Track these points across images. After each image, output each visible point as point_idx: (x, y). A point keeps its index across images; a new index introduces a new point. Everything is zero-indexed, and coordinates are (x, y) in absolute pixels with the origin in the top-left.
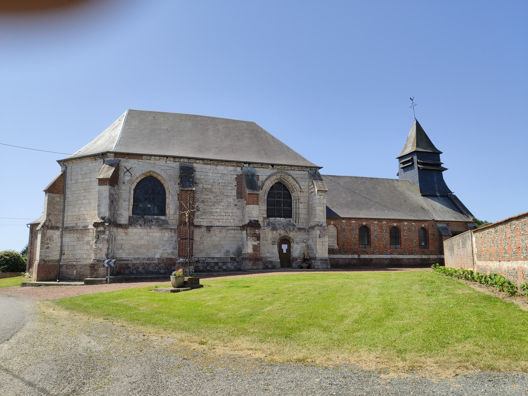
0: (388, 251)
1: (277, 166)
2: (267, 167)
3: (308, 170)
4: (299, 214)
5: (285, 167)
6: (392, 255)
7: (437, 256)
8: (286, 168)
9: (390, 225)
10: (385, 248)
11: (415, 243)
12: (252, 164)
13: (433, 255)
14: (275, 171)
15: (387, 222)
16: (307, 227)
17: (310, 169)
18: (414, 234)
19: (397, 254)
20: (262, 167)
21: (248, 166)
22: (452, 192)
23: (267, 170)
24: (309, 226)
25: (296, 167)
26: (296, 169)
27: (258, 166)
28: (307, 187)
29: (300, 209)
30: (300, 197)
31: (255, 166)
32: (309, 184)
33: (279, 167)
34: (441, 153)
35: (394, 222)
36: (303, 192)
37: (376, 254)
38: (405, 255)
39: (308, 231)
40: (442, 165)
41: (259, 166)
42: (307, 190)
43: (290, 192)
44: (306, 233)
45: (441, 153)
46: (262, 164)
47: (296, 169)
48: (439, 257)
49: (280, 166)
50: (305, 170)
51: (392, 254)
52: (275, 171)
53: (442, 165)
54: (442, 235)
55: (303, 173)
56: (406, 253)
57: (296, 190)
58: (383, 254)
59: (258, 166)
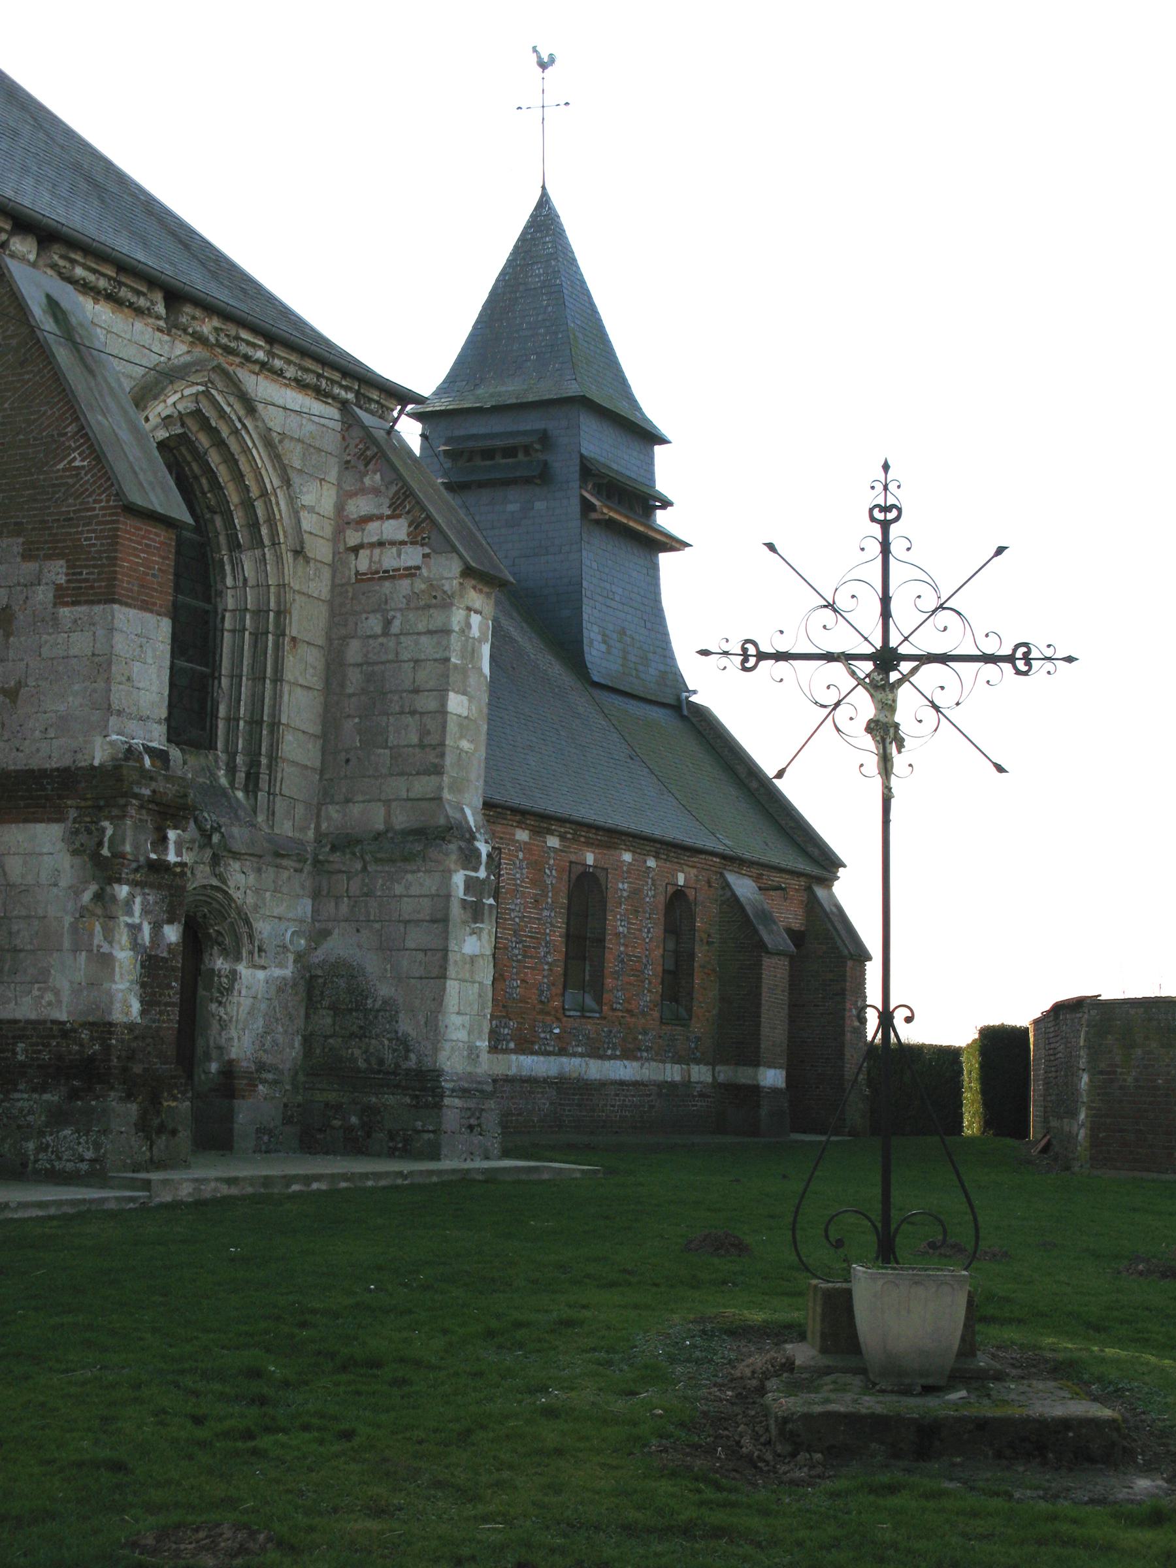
0: (551, 1032)
1: (198, 313)
2: (142, 302)
3: (350, 396)
4: (275, 725)
5: (245, 335)
6: (564, 1060)
7: (711, 1067)
8: (244, 348)
9: (573, 858)
10: (542, 1012)
11: (650, 983)
12: (63, 250)
13: (698, 1062)
14: (179, 351)
15: (562, 837)
16: (311, 834)
17: (358, 393)
18: (649, 932)
19: (582, 1055)
20: (110, 298)
21: (32, 257)
22: (691, 688)
23: (139, 325)
24: (324, 826)
25: (293, 358)
26: (291, 372)
27: (91, 278)
28: (328, 531)
29: (286, 688)
30: (289, 596)
31: (79, 272)
32: (340, 508)
33: (207, 327)
34: (663, 441)
35: (589, 844)
36: (307, 560)
37: (507, 1051)
38: (610, 1058)
39: (317, 862)
40: (662, 518)
41: (102, 283)
42: (320, 549)
43: (222, 539)
44: (304, 875)
45: (663, 441)
46: (124, 267)
47: (291, 372)
48: (721, 1078)
49: (216, 322)
50: (336, 390)
51: (562, 1052)
52: (179, 351)
53: (662, 518)
54: (761, 946)
55: (317, 407)
56: (614, 1049)
57: (274, 534)
58: (533, 1053)
59: (91, 278)
